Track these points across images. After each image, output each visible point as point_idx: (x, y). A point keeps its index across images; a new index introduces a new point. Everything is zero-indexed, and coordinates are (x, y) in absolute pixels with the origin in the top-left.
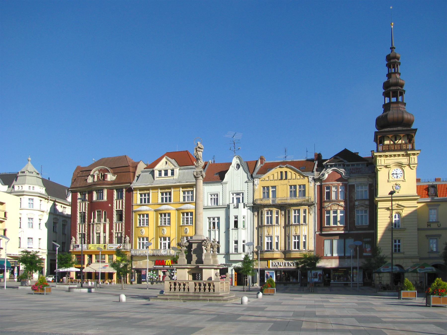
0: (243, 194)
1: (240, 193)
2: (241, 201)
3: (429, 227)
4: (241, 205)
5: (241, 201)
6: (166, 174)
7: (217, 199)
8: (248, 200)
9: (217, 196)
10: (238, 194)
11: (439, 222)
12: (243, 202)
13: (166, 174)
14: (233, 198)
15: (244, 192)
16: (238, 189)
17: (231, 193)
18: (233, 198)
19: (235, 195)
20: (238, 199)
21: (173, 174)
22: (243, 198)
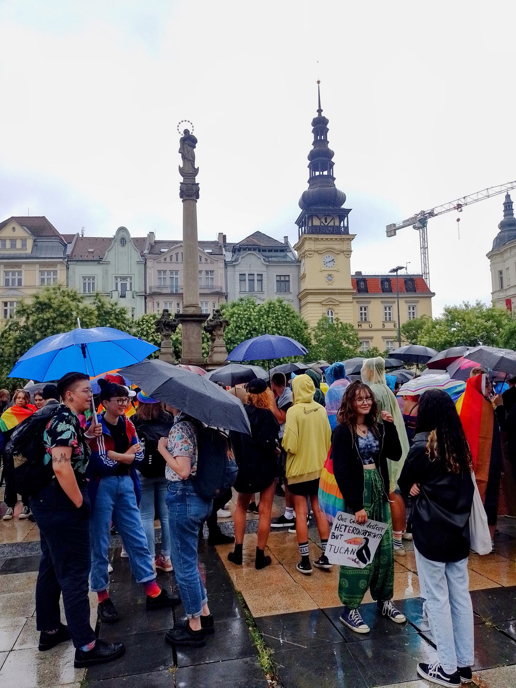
0: (131, 279)
1: (127, 277)
2: (128, 289)
3: (360, 327)
4: (129, 294)
5: (128, 289)
6: (13, 246)
7: (93, 283)
8: (138, 286)
9: (94, 278)
10: (124, 278)
11: (370, 322)
12: (131, 290)
13: (13, 246)
14: (117, 284)
15: (133, 276)
16: (123, 272)
17: (114, 276)
18: (117, 284)
19: (119, 279)
20: (124, 286)
21: (24, 245)
22: (131, 283)
